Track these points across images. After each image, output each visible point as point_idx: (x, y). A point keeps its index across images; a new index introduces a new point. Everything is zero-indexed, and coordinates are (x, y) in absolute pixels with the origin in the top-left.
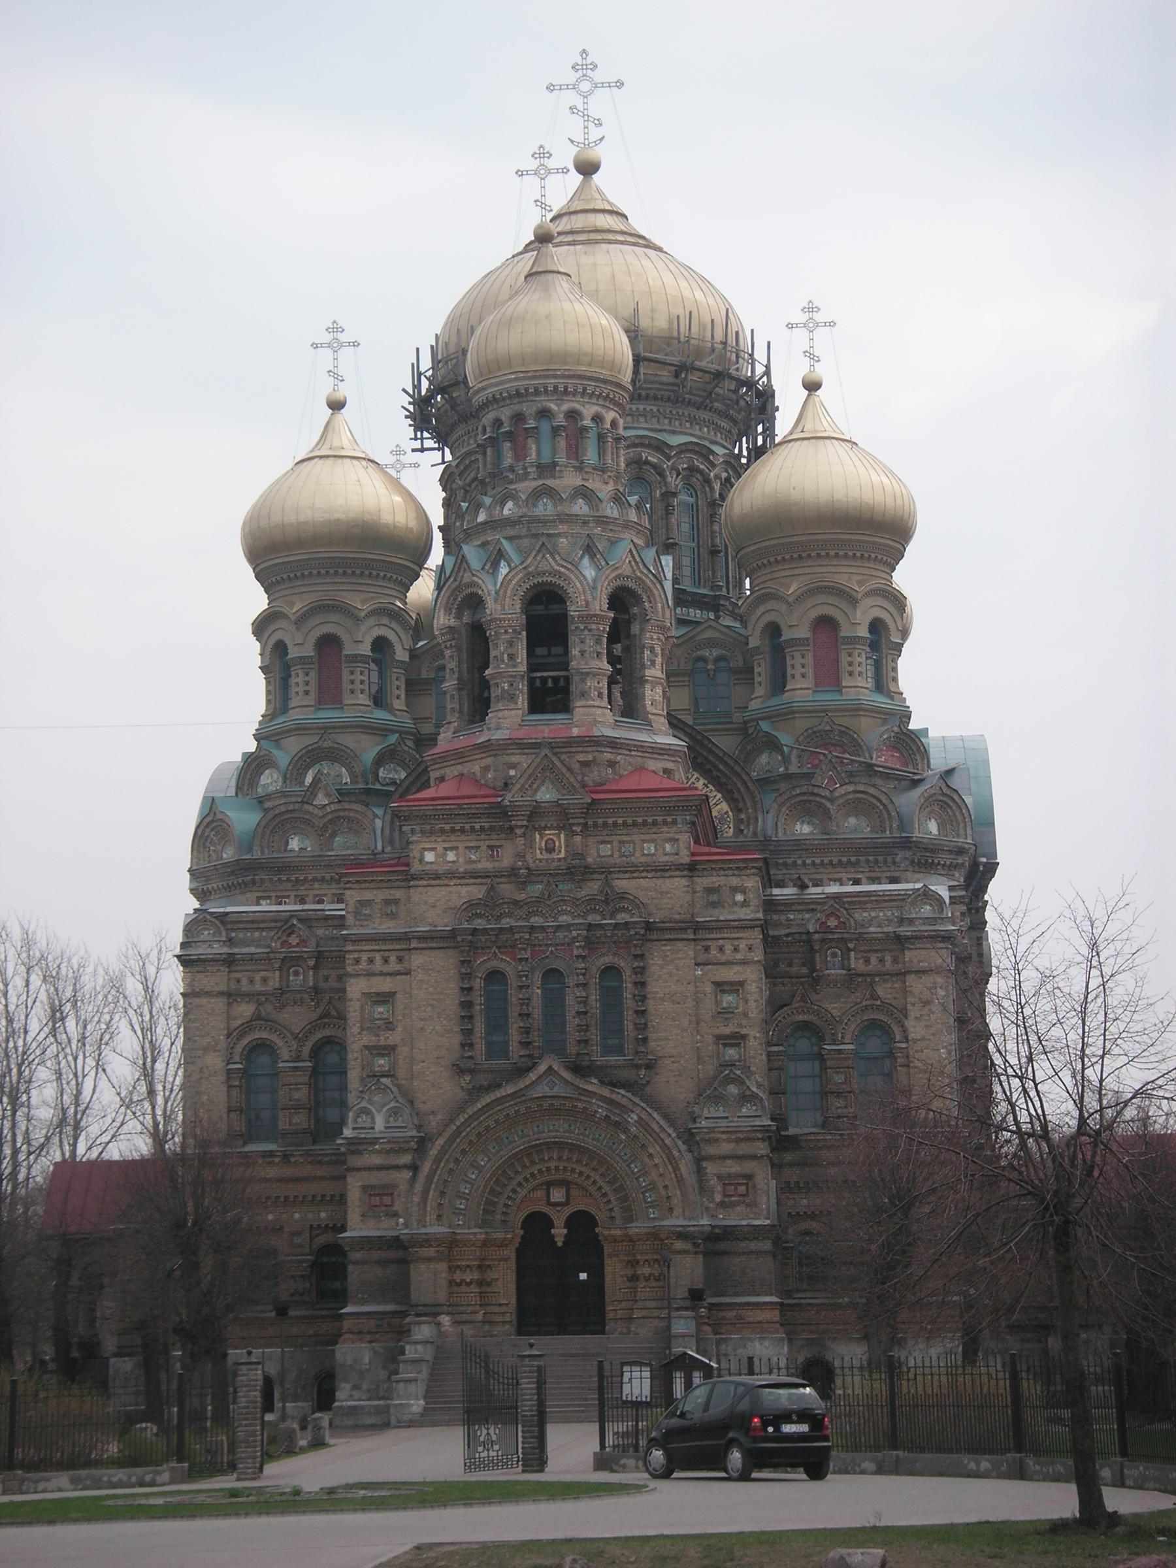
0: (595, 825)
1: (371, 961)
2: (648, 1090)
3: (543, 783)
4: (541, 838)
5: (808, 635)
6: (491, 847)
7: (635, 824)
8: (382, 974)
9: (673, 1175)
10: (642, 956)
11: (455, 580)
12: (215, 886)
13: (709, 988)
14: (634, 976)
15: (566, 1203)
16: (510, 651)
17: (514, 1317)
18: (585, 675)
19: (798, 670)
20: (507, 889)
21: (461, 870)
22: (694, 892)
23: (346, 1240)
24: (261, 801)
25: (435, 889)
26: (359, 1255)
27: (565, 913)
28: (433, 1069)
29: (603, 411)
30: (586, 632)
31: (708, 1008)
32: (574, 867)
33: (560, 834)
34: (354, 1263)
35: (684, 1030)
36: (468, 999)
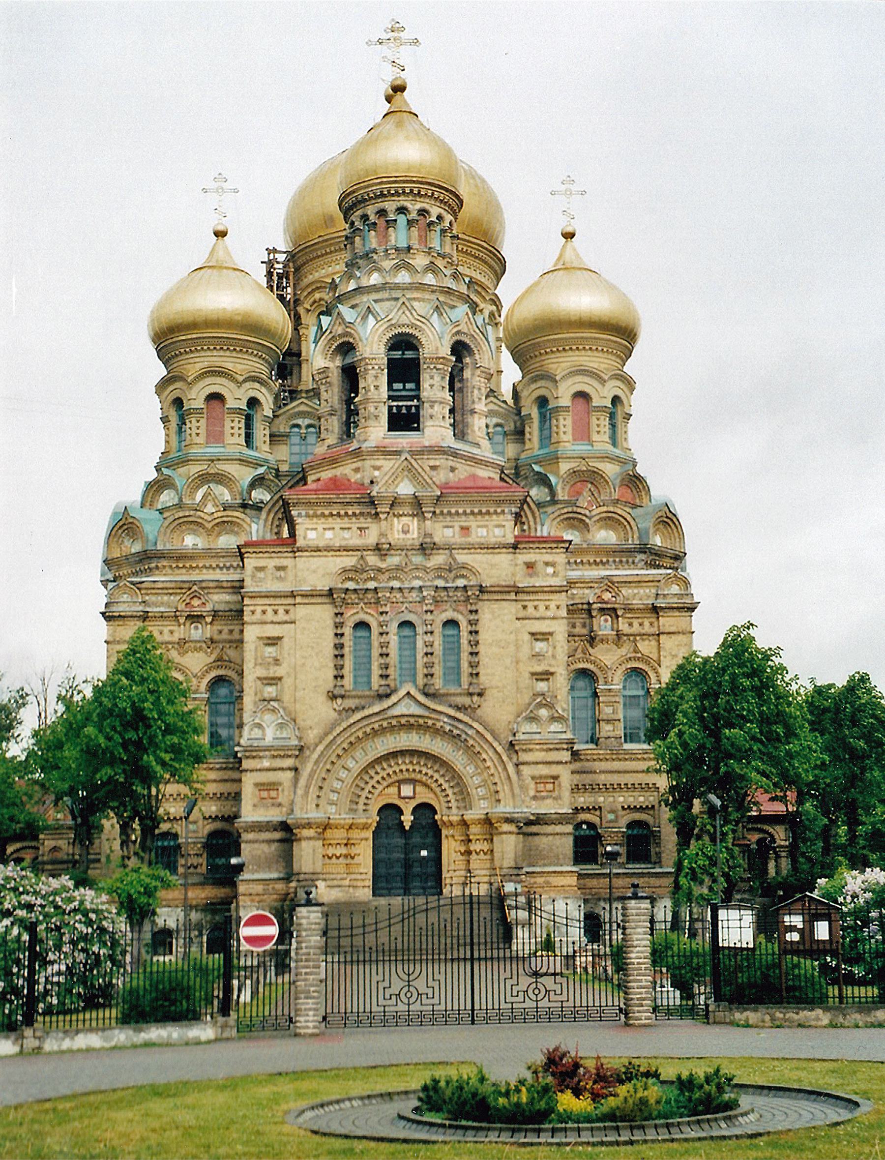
0: (442, 513)
1: (264, 612)
2: (478, 711)
3: (402, 481)
4: (399, 523)
5: (569, 404)
6: (360, 529)
7: (472, 513)
8: (272, 622)
10: (476, 611)
11: (331, 332)
12: (125, 572)
13: (527, 637)
14: (469, 627)
16: (375, 384)
18: (433, 403)
19: (562, 429)
20: (372, 560)
21: (337, 545)
22: (516, 565)
23: (241, 824)
24: (161, 512)
25: (315, 559)
26: (251, 836)
27: (417, 578)
29: (444, 213)
30: (435, 370)
31: (525, 652)
32: (426, 543)
33: (413, 521)
34: (246, 842)
35: (506, 668)
36: (342, 641)
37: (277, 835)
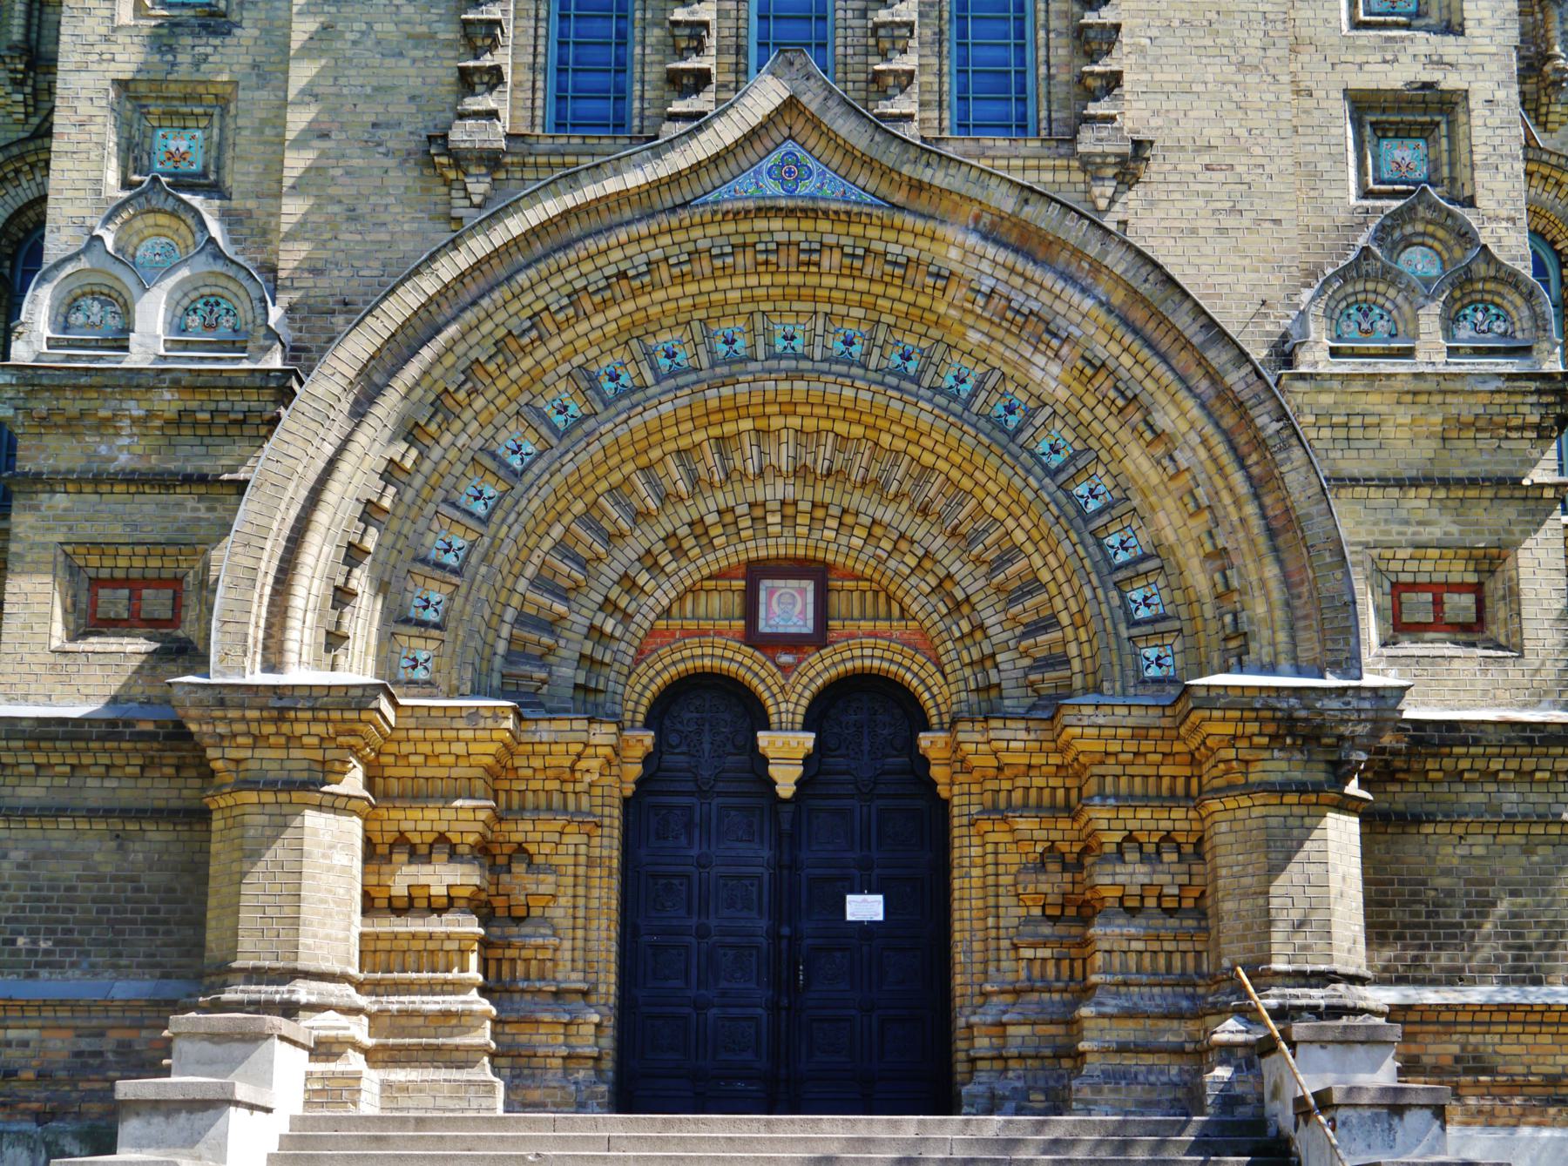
9: (1251, 509)
15: (820, 638)
17: (607, 1042)
28: (357, 162)
37: (160, 790)
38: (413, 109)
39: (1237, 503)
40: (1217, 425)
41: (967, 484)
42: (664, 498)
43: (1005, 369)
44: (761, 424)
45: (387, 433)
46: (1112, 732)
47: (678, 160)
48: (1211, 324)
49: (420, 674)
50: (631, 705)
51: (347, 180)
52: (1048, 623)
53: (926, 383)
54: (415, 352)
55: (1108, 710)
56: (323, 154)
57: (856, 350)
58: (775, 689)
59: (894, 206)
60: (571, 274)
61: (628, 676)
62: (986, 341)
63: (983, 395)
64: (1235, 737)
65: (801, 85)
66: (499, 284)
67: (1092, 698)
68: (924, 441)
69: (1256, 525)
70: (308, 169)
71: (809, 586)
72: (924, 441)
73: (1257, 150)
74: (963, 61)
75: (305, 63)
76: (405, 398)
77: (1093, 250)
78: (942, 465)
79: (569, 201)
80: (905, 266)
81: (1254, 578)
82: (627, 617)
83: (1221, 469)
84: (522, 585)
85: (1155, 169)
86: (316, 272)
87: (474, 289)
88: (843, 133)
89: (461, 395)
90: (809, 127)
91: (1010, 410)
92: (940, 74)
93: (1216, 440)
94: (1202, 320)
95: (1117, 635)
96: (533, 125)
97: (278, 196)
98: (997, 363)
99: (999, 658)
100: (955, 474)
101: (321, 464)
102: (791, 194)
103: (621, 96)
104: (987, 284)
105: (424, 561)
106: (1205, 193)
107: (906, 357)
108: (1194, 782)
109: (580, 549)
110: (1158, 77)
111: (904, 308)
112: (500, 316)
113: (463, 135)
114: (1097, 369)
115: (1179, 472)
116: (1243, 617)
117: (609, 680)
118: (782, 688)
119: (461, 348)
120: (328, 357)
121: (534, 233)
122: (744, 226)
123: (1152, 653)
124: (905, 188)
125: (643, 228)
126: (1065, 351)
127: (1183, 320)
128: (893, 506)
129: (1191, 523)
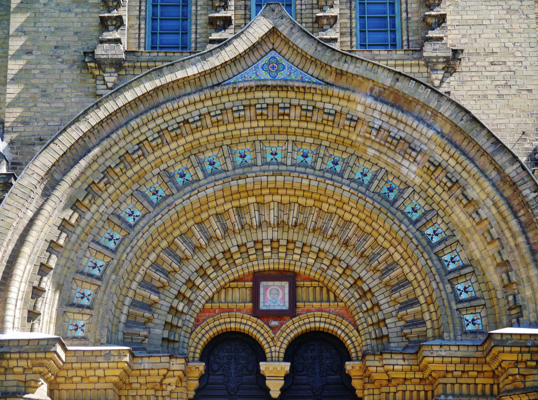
9: (521, 239)
28: (46, 66)
38: (76, 38)
39: (514, 236)
40: (502, 195)
41: (368, 229)
42: (209, 239)
43: (387, 168)
44: (260, 199)
45: (62, 205)
46: (450, 359)
47: (215, 61)
48: (497, 141)
49: (80, 333)
50: (192, 349)
51: (41, 76)
52: (413, 302)
53: (346, 176)
54: (77, 162)
55: (447, 348)
56: (29, 63)
57: (309, 160)
58: (269, 339)
59: (327, 84)
60: (159, 121)
61: (191, 334)
62: (377, 154)
63: (376, 182)
64: (517, 362)
65: (279, 22)
66: (121, 126)
67: (438, 342)
68: (346, 207)
69: (524, 248)
70: (21, 70)
71: (286, 284)
72: (346, 207)
73: (518, 54)
74: (362, 12)
75: (19, 15)
76: (71, 186)
77: (433, 104)
78: (355, 220)
79: (158, 83)
80: (334, 115)
81: (524, 276)
82: (190, 302)
83: (504, 218)
84: (134, 285)
85: (464, 65)
86: (25, 123)
87: (108, 129)
88: (301, 46)
89: (101, 185)
90: (283, 43)
91: (391, 190)
92: (351, 18)
93: (501, 203)
94: (492, 140)
95: (451, 307)
96: (139, 47)
97: (5, 84)
98: (383, 165)
99: (387, 321)
100: (362, 224)
101: (26, 222)
102: (274, 78)
103: (185, 33)
104: (378, 123)
105: (82, 273)
106: (491, 77)
107: (335, 163)
108: (495, 387)
109: (165, 266)
110: (465, 17)
111: (334, 137)
112: (122, 143)
113: (101, 51)
114: (436, 167)
115: (481, 221)
116: (519, 297)
117: (181, 335)
118: (273, 339)
119: (101, 160)
120: (30, 165)
121: (139, 99)
122: (250, 95)
123: (469, 317)
124: (334, 74)
125: (197, 97)
126: (419, 158)
127: (482, 140)
128: (330, 242)
129: (489, 247)
